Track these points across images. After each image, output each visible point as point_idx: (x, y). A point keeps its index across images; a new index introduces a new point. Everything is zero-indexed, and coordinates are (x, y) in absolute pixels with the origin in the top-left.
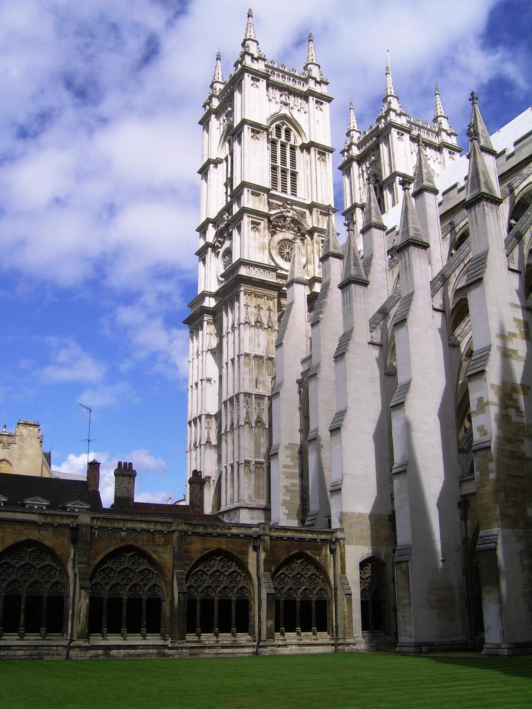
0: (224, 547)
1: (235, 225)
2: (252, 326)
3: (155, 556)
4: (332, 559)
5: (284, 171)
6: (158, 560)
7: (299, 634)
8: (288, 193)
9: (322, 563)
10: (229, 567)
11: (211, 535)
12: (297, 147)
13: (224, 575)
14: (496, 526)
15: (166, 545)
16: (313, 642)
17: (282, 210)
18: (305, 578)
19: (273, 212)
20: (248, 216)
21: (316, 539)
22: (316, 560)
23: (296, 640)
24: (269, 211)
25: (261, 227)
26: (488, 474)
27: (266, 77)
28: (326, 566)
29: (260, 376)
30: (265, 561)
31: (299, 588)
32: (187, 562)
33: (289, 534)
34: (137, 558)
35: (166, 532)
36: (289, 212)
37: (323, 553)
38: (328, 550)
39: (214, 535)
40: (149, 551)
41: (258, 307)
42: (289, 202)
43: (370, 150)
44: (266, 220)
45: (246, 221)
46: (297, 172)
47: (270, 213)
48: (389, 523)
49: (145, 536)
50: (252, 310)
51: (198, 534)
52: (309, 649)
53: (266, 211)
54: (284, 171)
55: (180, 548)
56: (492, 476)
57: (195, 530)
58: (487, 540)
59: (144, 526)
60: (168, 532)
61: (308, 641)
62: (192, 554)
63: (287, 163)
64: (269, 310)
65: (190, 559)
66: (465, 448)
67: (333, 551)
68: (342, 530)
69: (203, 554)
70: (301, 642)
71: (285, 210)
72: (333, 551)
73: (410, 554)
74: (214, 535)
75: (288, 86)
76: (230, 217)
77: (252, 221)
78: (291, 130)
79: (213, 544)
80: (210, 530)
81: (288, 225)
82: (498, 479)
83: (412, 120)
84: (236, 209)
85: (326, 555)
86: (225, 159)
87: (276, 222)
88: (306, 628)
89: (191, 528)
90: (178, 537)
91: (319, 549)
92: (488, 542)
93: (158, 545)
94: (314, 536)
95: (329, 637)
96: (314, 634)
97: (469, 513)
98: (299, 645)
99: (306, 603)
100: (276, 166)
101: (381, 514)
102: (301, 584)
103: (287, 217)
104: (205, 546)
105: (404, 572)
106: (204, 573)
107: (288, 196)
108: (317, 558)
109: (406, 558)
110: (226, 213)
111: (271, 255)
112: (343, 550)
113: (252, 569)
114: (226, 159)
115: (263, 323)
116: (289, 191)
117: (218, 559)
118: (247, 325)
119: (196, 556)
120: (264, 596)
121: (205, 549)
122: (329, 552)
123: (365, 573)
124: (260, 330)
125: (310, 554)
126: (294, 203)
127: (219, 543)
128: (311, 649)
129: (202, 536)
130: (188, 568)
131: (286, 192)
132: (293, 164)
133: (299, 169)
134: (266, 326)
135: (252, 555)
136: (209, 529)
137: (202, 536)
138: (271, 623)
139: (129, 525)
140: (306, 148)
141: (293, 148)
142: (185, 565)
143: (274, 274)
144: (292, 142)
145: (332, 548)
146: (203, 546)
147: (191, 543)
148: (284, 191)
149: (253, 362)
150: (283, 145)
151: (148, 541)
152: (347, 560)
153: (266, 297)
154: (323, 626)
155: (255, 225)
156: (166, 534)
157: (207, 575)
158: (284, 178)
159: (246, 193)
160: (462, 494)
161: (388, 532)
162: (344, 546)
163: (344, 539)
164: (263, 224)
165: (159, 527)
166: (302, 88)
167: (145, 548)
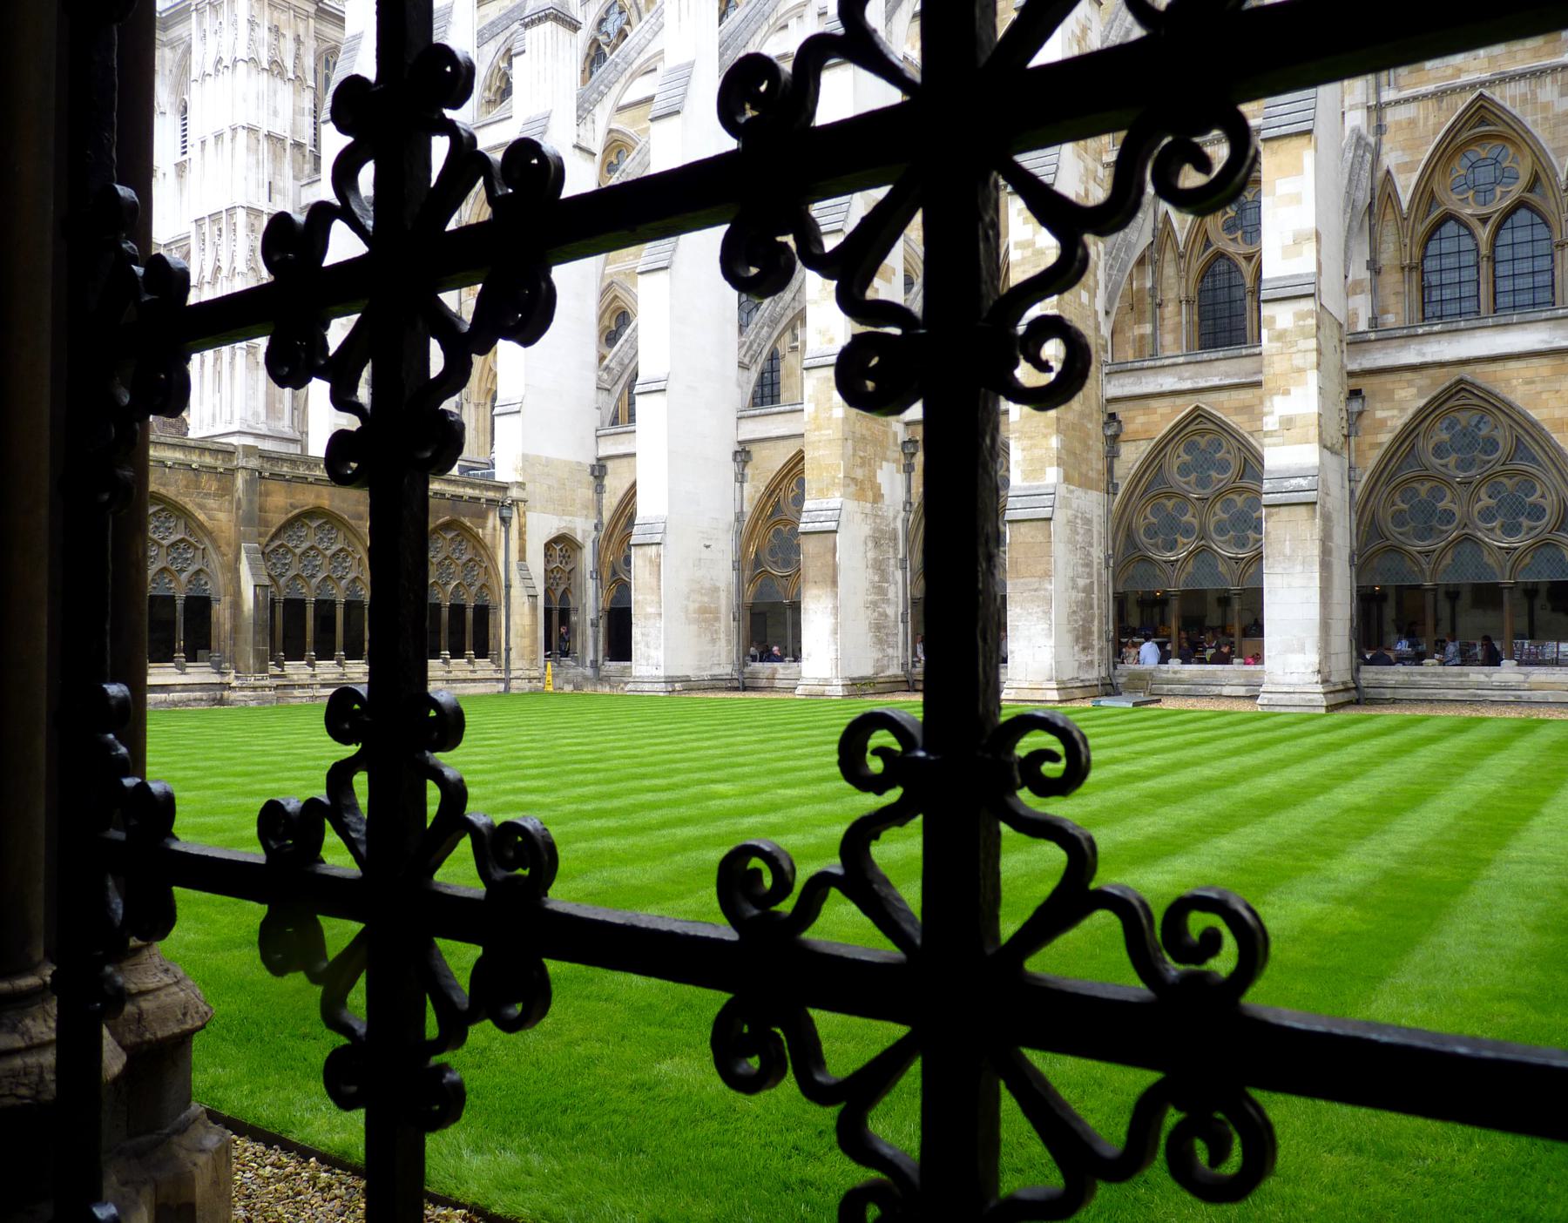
2: (263, 69)
3: (201, 517)
4: (503, 535)
6: (207, 523)
7: (446, 662)
9: (488, 540)
10: (332, 541)
11: (303, 480)
13: (325, 556)
14: (838, 494)
15: (223, 496)
16: (470, 676)
18: (457, 565)
21: (479, 499)
22: (478, 534)
23: (442, 673)
26: (831, 408)
28: (494, 547)
29: (278, 177)
31: (447, 583)
32: (262, 529)
34: (162, 519)
35: (222, 470)
38: (498, 519)
39: (309, 480)
40: (190, 506)
41: (275, 30)
48: (592, 478)
49: (181, 477)
50: (263, 33)
51: (279, 477)
52: (462, 687)
55: (250, 502)
57: (276, 470)
58: (822, 515)
60: (225, 469)
61: (461, 675)
62: (270, 516)
64: (297, 39)
65: (265, 523)
66: (746, 360)
67: (505, 521)
68: (521, 485)
69: (290, 515)
70: (451, 676)
72: (505, 521)
73: (664, 532)
74: (309, 480)
80: (302, 471)
85: (494, 528)
88: (457, 653)
89: (267, 466)
90: (249, 483)
91: (482, 516)
92: (822, 519)
93: (207, 495)
94: (476, 493)
95: (493, 667)
96: (470, 662)
97: (748, 471)
98: (447, 681)
99: (458, 610)
101: (579, 463)
102: (451, 576)
104: (292, 501)
105: (651, 561)
106: (289, 551)
108: (480, 531)
109: (657, 538)
112: (523, 520)
115: (286, 68)
117: (314, 525)
118: (252, 65)
119: (278, 519)
121: (293, 506)
122: (498, 522)
123: (567, 563)
124: (278, 81)
125: (468, 524)
127: (318, 496)
128: (466, 688)
129: (287, 480)
130: (264, 540)
134: (291, 76)
136: (301, 469)
137: (287, 480)
142: (260, 535)
145: (504, 515)
146: (289, 501)
147: (267, 494)
149: (264, 144)
151: (187, 487)
152: (528, 537)
153: (292, 12)
154: (482, 651)
156: (221, 473)
157: (294, 554)
160: (740, 439)
161: (589, 493)
162: (524, 513)
163: (525, 502)
165: (208, 460)
167: (182, 500)
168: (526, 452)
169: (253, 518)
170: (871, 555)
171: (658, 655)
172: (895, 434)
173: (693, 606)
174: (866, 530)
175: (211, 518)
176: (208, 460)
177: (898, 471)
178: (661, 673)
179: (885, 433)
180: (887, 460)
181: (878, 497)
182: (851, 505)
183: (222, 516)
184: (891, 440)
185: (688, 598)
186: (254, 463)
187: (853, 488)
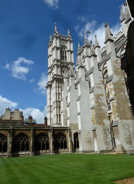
0: (43, 132)
3: (28, 135)
6: (28, 136)
9: (65, 134)
30: (52, 134)
33: (57, 128)
37: (65, 132)
54: (64, 56)
56: (95, 114)
59: (25, 128)
68: (69, 127)
72: (67, 132)
79: (41, 132)
82: (96, 114)
88: (62, 148)
94: (63, 129)
107: (65, 61)
111: (61, 73)
113: (49, 136)
120: (52, 142)
122: (67, 132)
132: (65, 55)
135: (49, 133)
138: (53, 147)
139: (22, 128)
140: (68, 51)
141: (65, 52)
150: (63, 51)
155: (58, 68)
158: (64, 58)
165: (28, 128)
168: (71, 123)
169: (34, 134)
170: (103, 132)
171: (81, 148)
172: (107, 115)
173: (87, 141)
174: (102, 129)
175: (29, 135)
176: (28, 128)
177: (108, 120)
178: (82, 150)
179: (105, 115)
180: (105, 119)
181: (104, 124)
182: (98, 126)
183: (30, 134)
184: (106, 116)
185: (86, 140)
186: (33, 128)
187: (98, 123)
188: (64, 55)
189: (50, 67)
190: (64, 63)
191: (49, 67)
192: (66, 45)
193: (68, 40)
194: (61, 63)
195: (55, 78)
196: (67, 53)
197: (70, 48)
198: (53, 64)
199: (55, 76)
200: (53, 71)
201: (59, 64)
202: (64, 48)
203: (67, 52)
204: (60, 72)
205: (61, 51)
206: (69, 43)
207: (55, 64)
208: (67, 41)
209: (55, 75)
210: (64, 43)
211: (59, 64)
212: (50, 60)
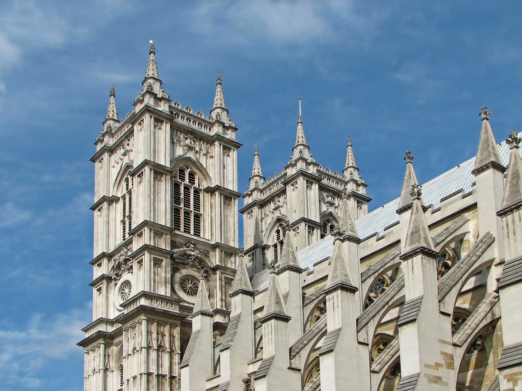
1: (136, 260)
5: (187, 213)
8: (191, 233)
12: (202, 190)
17: (185, 249)
19: (175, 250)
20: (151, 253)
24: (171, 249)
25: (164, 263)
27: (170, 118)
36: (192, 251)
42: (193, 242)
43: (275, 196)
44: (169, 256)
45: (146, 257)
46: (202, 215)
47: (173, 251)
53: (170, 250)
54: (187, 213)
63: (191, 204)
71: (188, 249)
75: (194, 130)
76: (129, 253)
77: (154, 257)
78: (196, 174)
81: (191, 263)
83: (322, 169)
84: (136, 246)
86: (121, 197)
87: (179, 260)
100: (179, 207)
103: (191, 255)
107: (191, 235)
110: (125, 249)
114: (124, 197)
116: (192, 232)
126: (195, 244)
131: (190, 232)
132: (197, 206)
133: (205, 210)
140: (211, 191)
143: (178, 307)
144: (196, 185)
148: (187, 231)
150: (187, 188)
155: (157, 263)
159: (146, 231)
164: (166, 262)
166: (208, 133)
188: (187, 205)
189: (110, 256)
190: (189, 241)
191: (104, 255)
192: (203, 161)
193: (219, 138)
194: (174, 245)
195: (143, 309)
196: (205, 199)
197: (223, 177)
198: (127, 244)
199: (143, 302)
200: (126, 277)
201: (164, 244)
202: (192, 175)
203: (208, 196)
204: (169, 286)
205: (176, 186)
206: (217, 149)
207: (145, 248)
208: (210, 141)
209: (144, 295)
210: (191, 148)
211: (164, 244)
212: (108, 223)
